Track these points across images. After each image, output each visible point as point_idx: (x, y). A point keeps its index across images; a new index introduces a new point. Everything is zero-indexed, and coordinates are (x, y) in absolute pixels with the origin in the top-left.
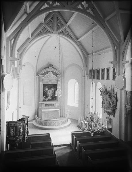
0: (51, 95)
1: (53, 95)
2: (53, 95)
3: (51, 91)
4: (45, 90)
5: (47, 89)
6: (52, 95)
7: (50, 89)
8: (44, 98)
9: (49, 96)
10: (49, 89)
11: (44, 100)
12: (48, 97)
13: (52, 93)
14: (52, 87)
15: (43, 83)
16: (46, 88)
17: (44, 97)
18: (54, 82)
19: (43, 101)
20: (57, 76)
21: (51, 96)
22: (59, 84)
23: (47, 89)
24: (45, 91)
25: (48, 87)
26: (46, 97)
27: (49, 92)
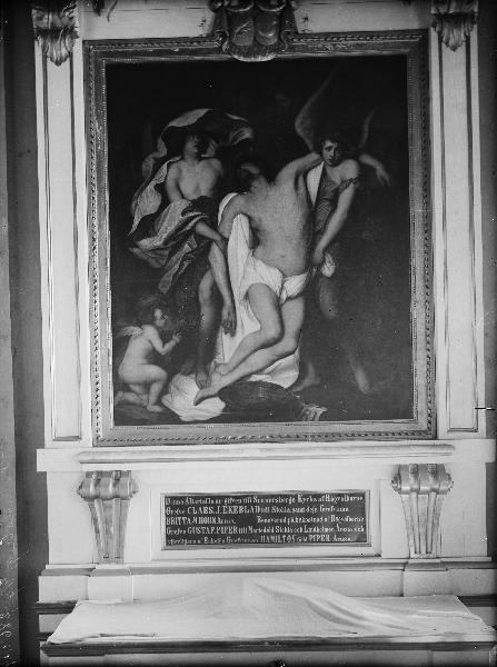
0: (278, 305)
1: (326, 298)
2: (326, 298)
3: (280, 206)
4: (148, 202)
6: (309, 294)
7: (271, 178)
8: (136, 367)
9: (250, 324)
10: (233, 181)
12: (228, 347)
13: (310, 265)
14: (300, 126)
16: (176, 151)
17: (145, 338)
19: (124, 415)
21: (295, 314)
24: (149, 225)
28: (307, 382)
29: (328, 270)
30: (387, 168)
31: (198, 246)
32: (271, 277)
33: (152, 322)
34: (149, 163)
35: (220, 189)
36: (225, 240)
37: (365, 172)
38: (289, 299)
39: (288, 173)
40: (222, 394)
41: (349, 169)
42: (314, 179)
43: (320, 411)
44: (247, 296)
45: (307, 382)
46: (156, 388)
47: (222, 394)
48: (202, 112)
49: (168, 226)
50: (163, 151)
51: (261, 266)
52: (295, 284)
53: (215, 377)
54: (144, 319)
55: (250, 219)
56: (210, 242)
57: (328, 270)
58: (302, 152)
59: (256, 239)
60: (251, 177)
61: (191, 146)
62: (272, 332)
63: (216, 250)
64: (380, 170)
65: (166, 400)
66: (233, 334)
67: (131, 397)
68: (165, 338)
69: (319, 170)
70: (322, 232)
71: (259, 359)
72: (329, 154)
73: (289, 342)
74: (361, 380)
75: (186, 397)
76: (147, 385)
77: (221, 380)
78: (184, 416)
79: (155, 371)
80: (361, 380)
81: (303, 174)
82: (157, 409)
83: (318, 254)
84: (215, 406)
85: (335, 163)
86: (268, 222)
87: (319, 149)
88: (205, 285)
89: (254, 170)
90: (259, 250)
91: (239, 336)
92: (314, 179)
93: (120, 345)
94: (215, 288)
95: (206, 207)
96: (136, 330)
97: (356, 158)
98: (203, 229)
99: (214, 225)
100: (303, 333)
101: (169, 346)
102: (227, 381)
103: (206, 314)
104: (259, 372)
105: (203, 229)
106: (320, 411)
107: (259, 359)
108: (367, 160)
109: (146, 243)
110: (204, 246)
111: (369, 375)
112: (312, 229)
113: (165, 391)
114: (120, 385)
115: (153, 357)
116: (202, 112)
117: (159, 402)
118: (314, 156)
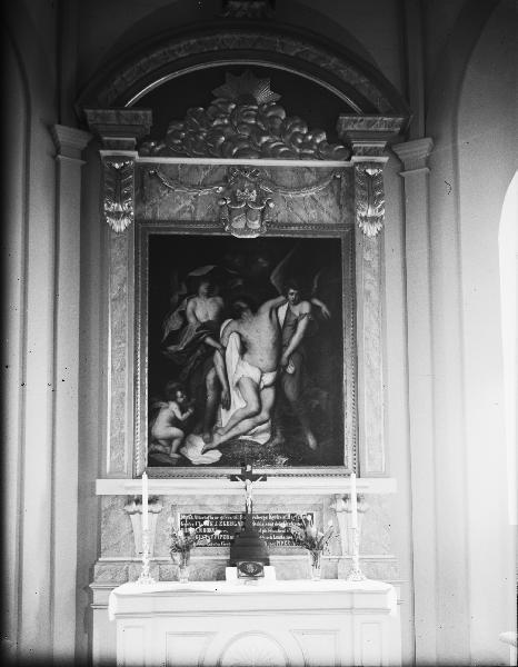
0: (258, 390)
1: (290, 390)
2: (290, 390)
3: (261, 331)
4: (174, 323)
5: (203, 309)
6: (277, 385)
7: (255, 311)
8: (163, 429)
9: (241, 402)
10: (230, 312)
11: (162, 459)
12: (225, 417)
13: (279, 367)
15: (139, 221)
16: (193, 293)
17: (171, 409)
18: (308, 210)
20: (334, 138)
21: (268, 396)
22: (371, 230)
23: (203, 309)
24: (175, 337)
25: (219, 286)
26: (200, 420)
27: (233, 344)
28: (277, 441)
29: (290, 370)
30: (328, 308)
31: (204, 350)
32: (255, 375)
34: (176, 298)
35: (222, 316)
36: (224, 349)
37: (315, 309)
38: (265, 387)
39: (265, 309)
40: (220, 447)
41: (305, 307)
42: (282, 312)
43: (284, 460)
44: (238, 385)
45: (277, 441)
46: (176, 443)
47: (220, 447)
48: (211, 267)
49: (187, 338)
50: (184, 290)
51: (246, 364)
52: (269, 378)
53: (216, 436)
54: (171, 398)
55: (240, 336)
56: (215, 349)
57: (290, 370)
58: (275, 295)
59: (244, 348)
60: (242, 309)
61: (203, 289)
62: (254, 407)
63: (218, 355)
64: (324, 309)
65: (183, 450)
66: (228, 407)
67: (160, 448)
68: (183, 411)
69: (285, 307)
70: (287, 346)
71: (247, 424)
72: (291, 297)
73: (264, 415)
74: (312, 442)
75: (196, 450)
76: (170, 440)
77: (219, 439)
78: (195, 461)
79: (175, 431)
80: (312, 442)
81: (275, 309)
82: (176, 456)
83: (284, 360)
84: (216, 455)
85: (296, 303)
86: (251, 336)
87: (286, 294)
88: (211, 376)
89: (244, 305)
90: (246, 356)
91: (232, 411)
92: (282, 312)
93: (153, 414)
94: (217, 379)
95: (212, 329)
96: (165, 404)
97: (309, 300)
98: (209, 341)
99: (217, 338)
100: (272, 411)
102: (224, 439)
103: (211, 397)
104: (245, 434)
105: (209, 341)
106: (284, 460)
107: (247, 424)
109: (172, 348)
110: (211, 351)
111: (316, 436)
112: (280, 344)
113: (183, 444)
114: (152, 440)
115: (174, 422)
116: (211, 267)
117: (178, 452)
118: (282, 298)
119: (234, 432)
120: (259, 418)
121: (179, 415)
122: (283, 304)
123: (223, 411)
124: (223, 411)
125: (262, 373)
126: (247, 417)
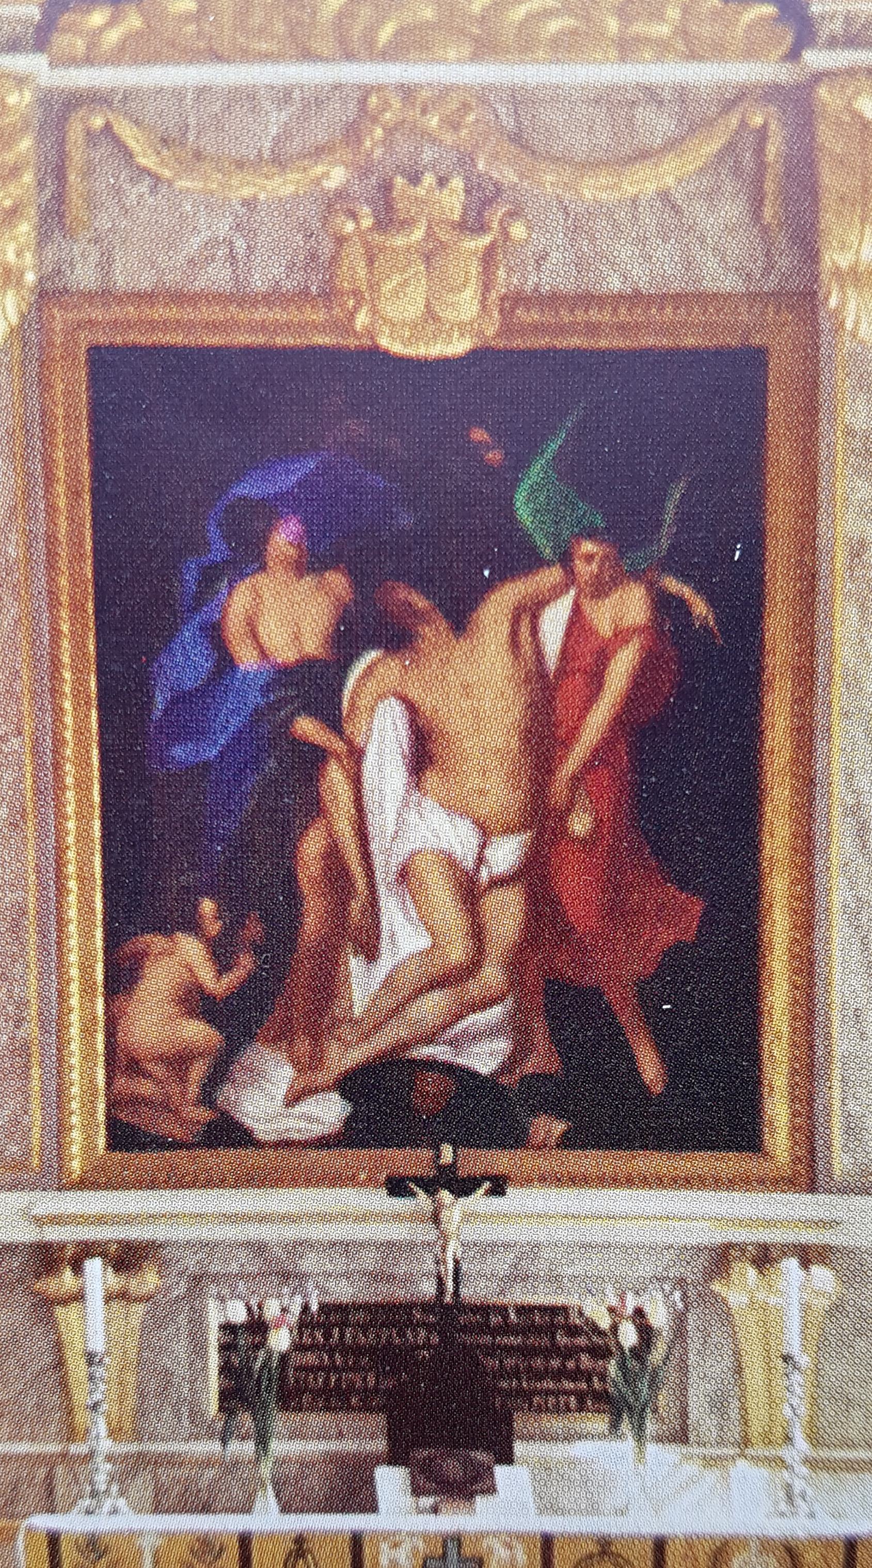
33: (192, 925)
38: (498, 882)
43: (559, 1127)
44: (404, 875)
46: (198, 1071)
53: (333, 1050)
55: (412, 709)
66: (371, 953)
67: (146, 1088)
68: (222, 965)
78: (263, 1130)
87: (565, 559)
96: (157, 942)
101: (231, 979)
102: (356, 1056)
104: (430, 1039)
106: (559, 1127)
108: (673, 585)
118: (552, 575)
119: (382, 1041)
120: (474, 989)
121: (206, 975)
122: (557, 592)
123: (355, 964)
124: (355, 964)
125: (486, 832)
126: (435, 984)
